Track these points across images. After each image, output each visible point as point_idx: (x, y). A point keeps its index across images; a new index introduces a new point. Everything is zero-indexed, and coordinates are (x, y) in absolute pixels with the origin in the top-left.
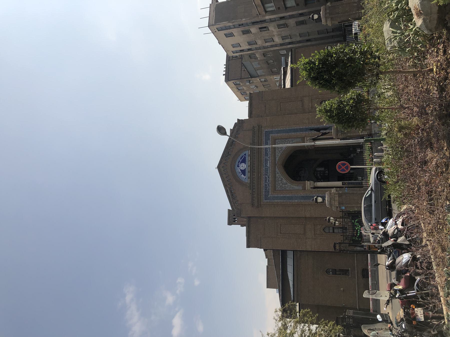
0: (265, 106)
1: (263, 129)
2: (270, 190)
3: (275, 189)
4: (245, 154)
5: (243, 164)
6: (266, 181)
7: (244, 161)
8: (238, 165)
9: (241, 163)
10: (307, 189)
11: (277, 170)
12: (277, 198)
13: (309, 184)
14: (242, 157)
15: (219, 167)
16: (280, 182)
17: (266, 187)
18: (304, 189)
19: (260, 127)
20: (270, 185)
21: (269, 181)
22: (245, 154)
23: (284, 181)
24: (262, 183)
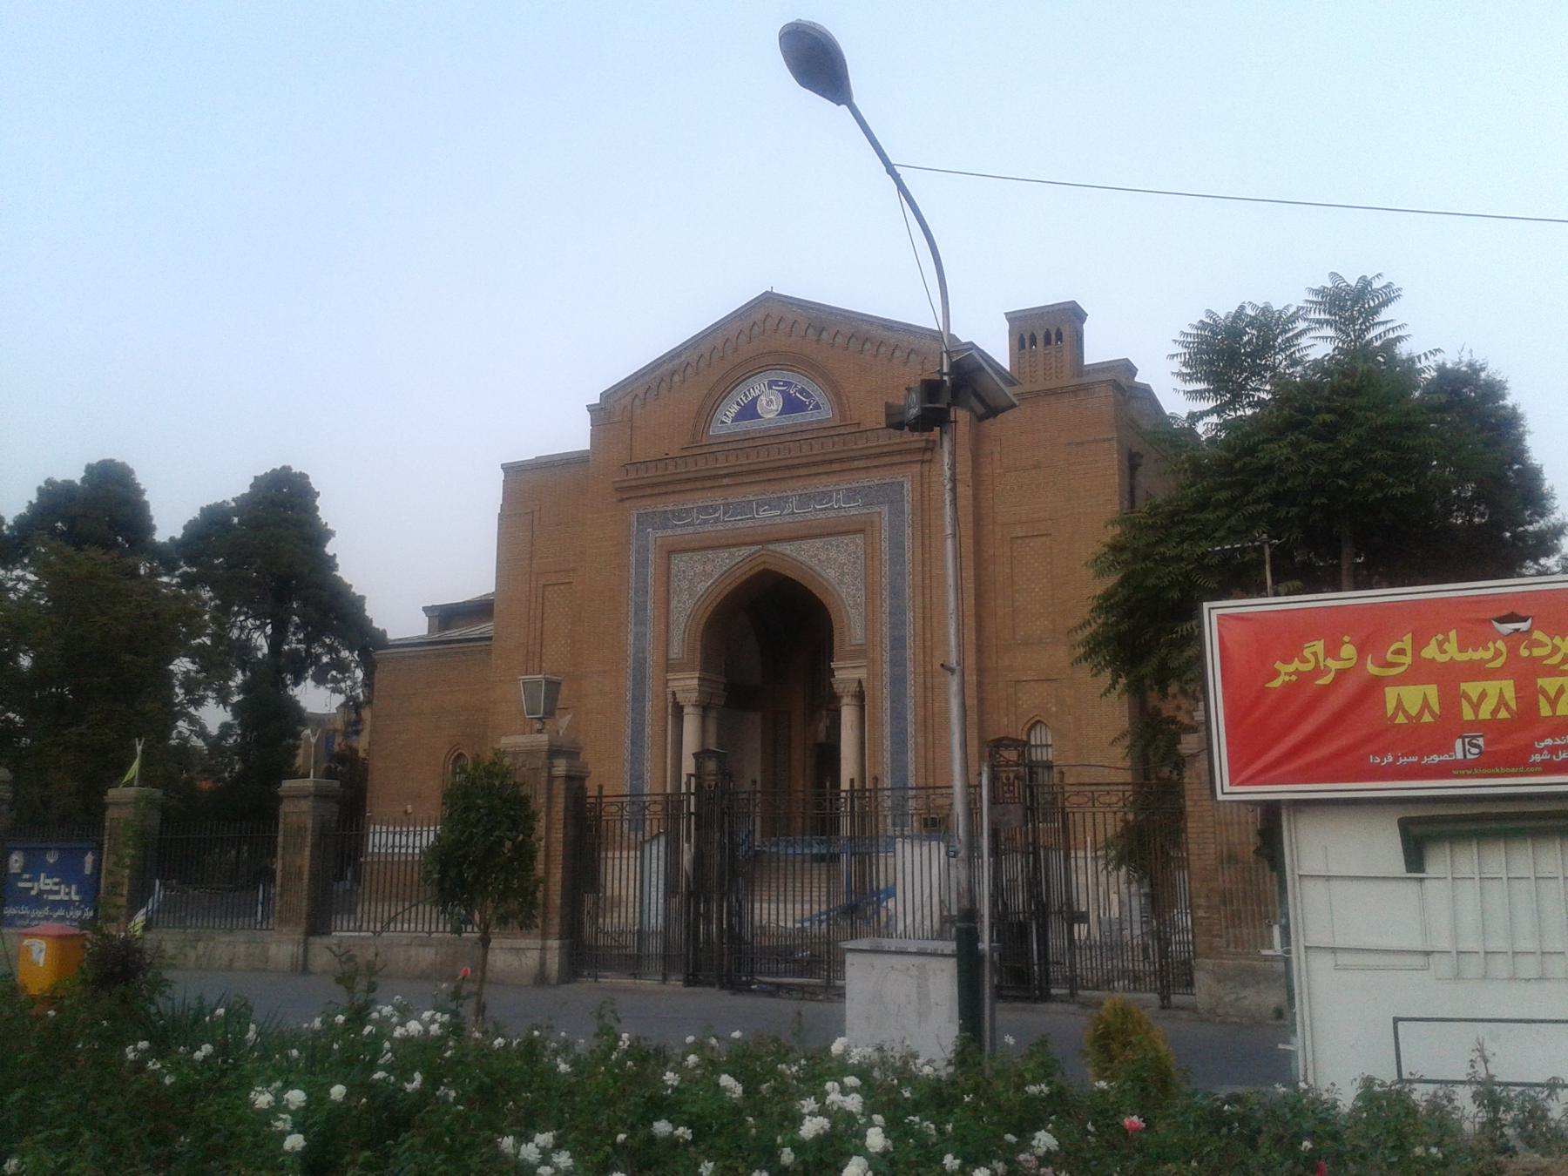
0: (1037, 466)
1: (916, 468)
2: (670, 532)
3: (670, 552)
4: (817, 407)
5: (777, 405)
6: (703, 510)
7: (791, 405)
8: (776, 383)
9: (787, 397)
10: (670, 676)
11: (745, 551)
12: (642, 563)
13: (687, 684)
14: (808, 395)
15: (768, 300)
16: (699, 568)
17: (678, 515)
18: (669, 666)
19: (928, 456)
20: (690, 530)
21: (705, 522)
22: (817, 407)
23: (702, 586)
24: (698, 495)
